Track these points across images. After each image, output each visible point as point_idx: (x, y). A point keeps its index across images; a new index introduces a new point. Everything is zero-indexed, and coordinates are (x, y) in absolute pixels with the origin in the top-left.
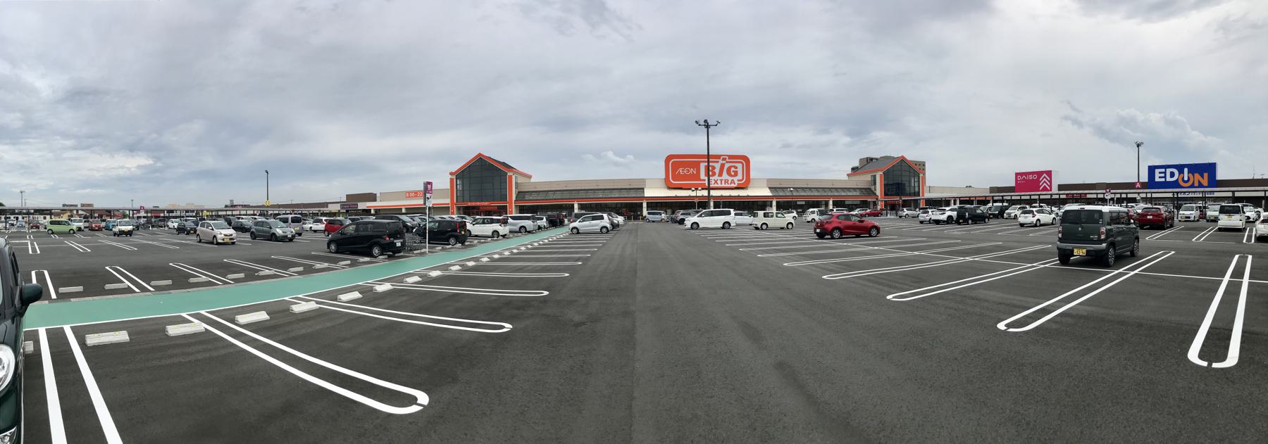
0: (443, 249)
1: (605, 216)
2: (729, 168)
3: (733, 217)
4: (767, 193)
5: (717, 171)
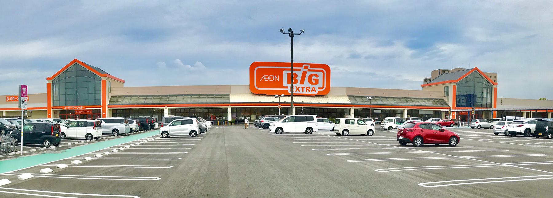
0: (38, 151)
1: (194, 120)
2: (310, 77)
3: (316, 124)
4: (345, 100)
5: (299, 78)
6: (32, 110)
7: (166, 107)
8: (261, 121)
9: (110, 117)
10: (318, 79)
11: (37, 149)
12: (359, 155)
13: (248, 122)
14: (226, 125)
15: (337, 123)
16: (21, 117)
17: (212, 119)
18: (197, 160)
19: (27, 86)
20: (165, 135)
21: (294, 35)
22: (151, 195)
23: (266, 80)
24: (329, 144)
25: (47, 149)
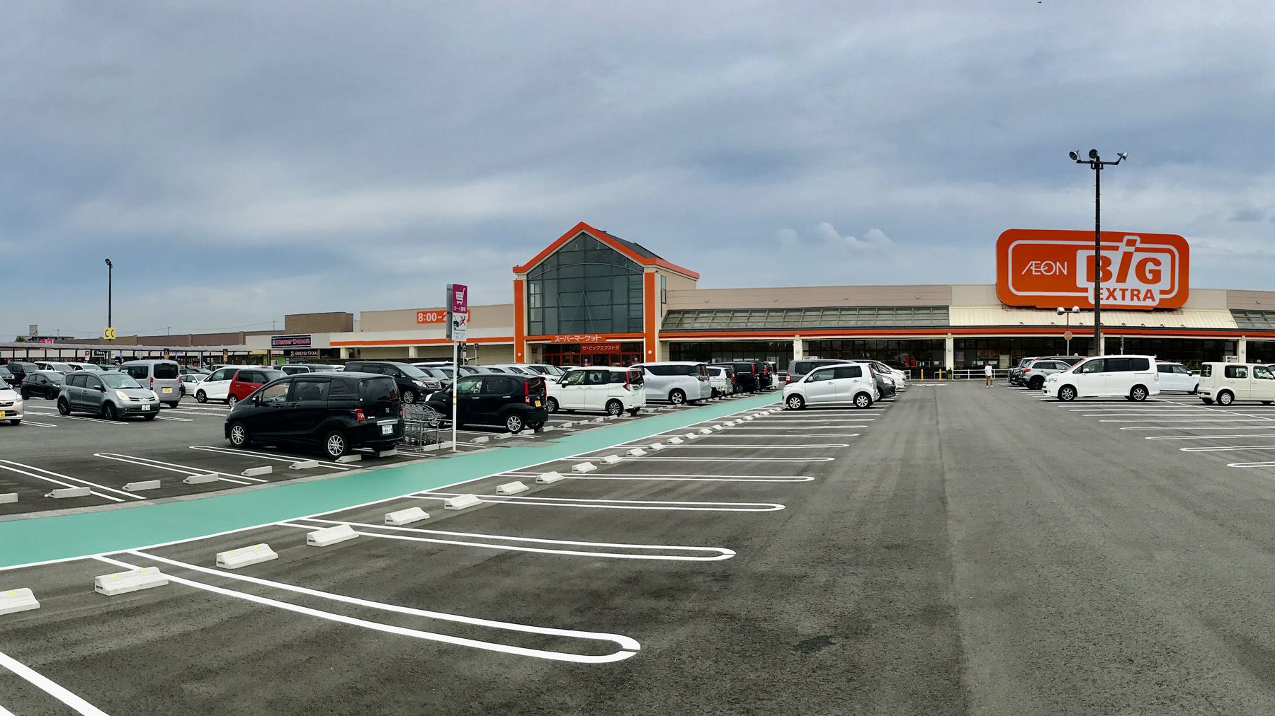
0: (492, 442)
1: (865, 367)
2: (1142, 265)
3: (1154, 377)
4: (1225, 321)
5: (1114, 268)
6: (480, 344)
7: (797, 337)
8: (1023, 369)
9: (663, 360)
10: (1160, 271)
11: (491, 438)
12: (1257, 452)
13: (993, 372)
14: (940, 379)
15: (1205, 376)
16: (452, 359)
17: (908, 366)
18: (872, 463)
19: (466, 287)
20: (795, 402)
21: (1102, 166)
22: (762, 547)
23: (1036, 271)
24: (1185, 424)
25: (515, 436)
